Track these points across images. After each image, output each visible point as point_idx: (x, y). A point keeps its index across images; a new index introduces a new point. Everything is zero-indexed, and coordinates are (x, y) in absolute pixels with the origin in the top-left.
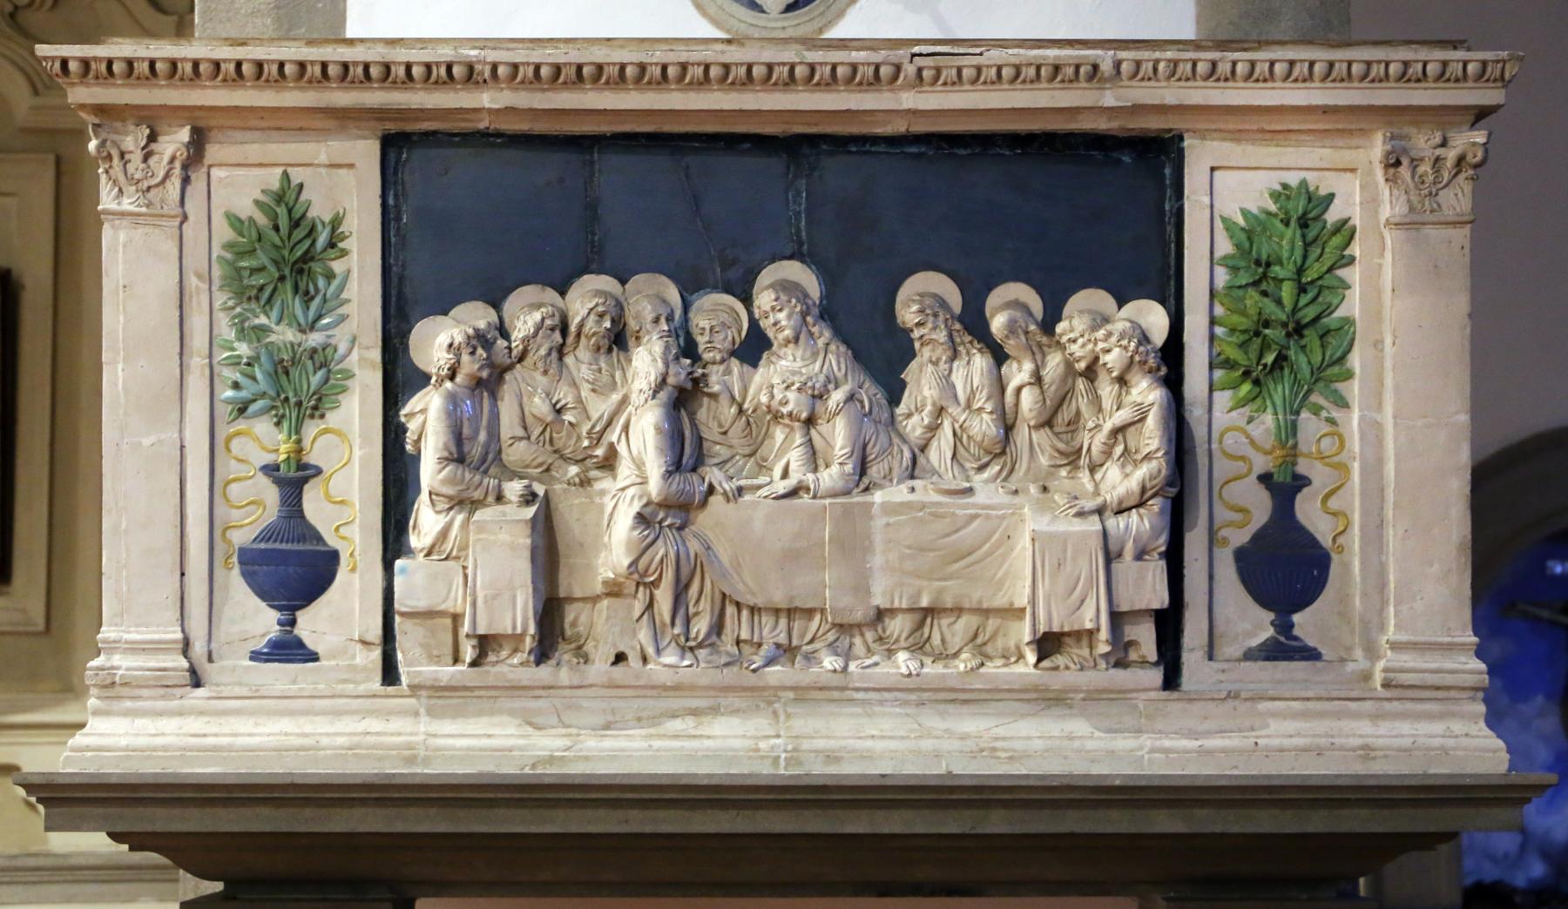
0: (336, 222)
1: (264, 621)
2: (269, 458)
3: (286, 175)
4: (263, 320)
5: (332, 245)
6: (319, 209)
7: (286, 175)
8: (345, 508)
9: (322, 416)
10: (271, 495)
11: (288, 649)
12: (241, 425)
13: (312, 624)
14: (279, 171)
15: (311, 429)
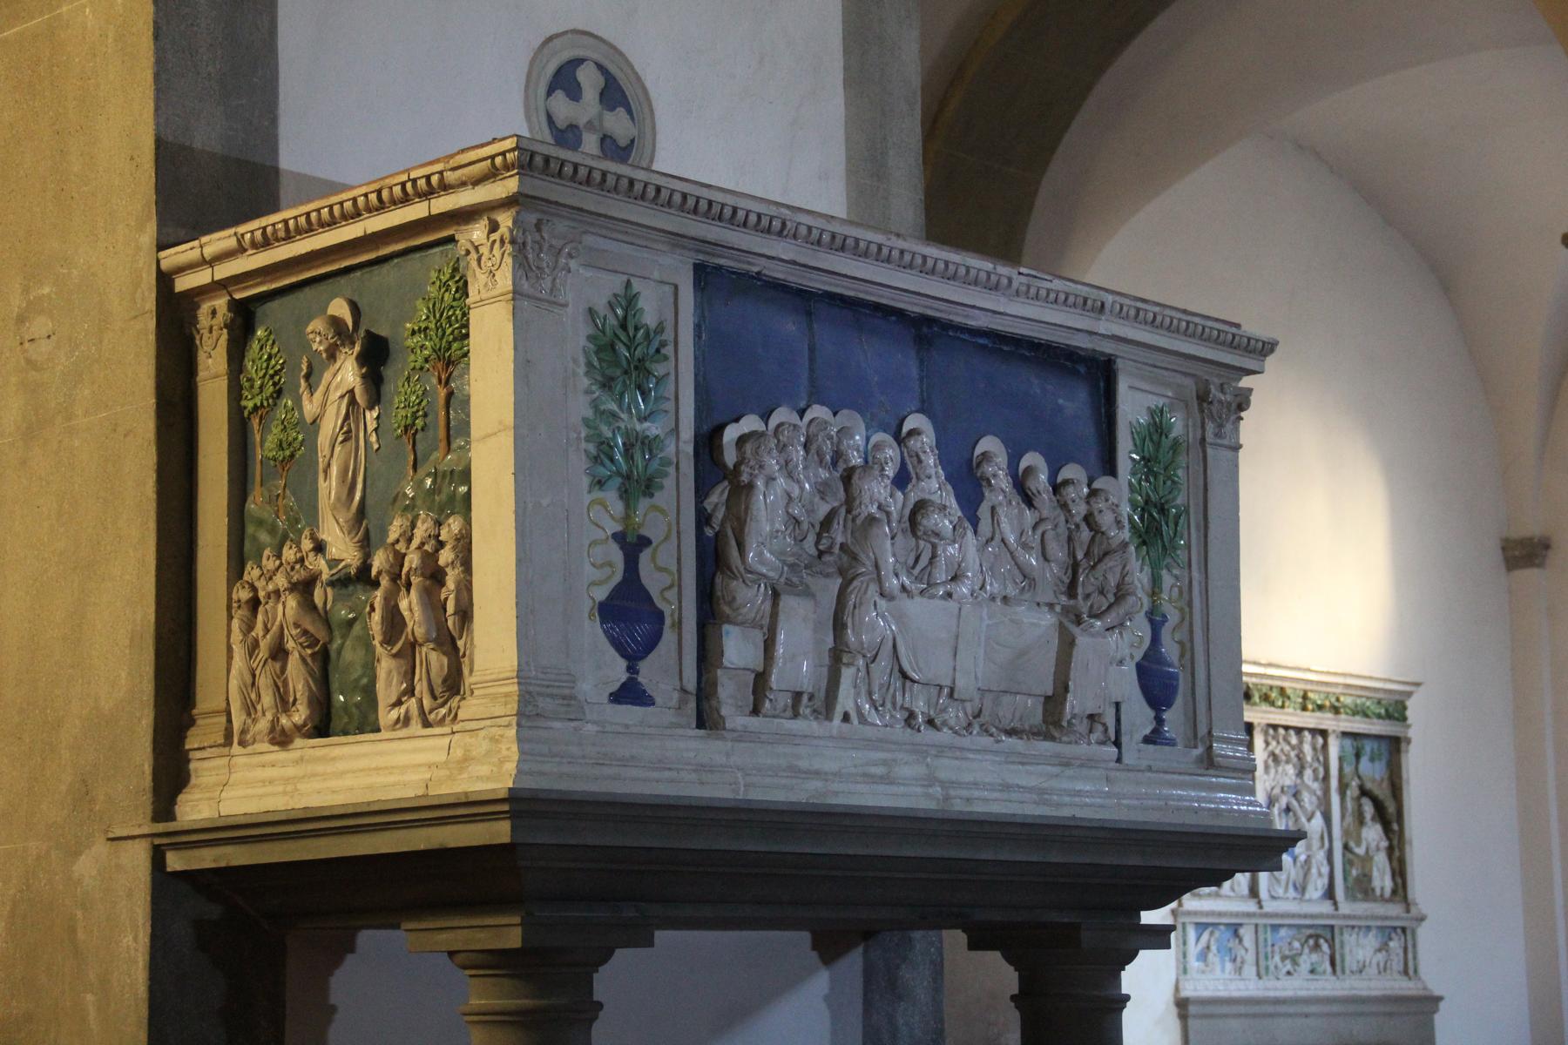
0: (660, 329)
1: (617, 671)
2: (618, 528)
3: (628, 284)
4: (614, 407)
5: (658, 351)
6: (649, 319)
7: (628, 284)
8: (670, 576)
9: (652, 495)
10: (617, 556)
11: (631, 693)
12: (598, 494)
13: (651, 673)
14: (625, 278)
15: (644, 504)
